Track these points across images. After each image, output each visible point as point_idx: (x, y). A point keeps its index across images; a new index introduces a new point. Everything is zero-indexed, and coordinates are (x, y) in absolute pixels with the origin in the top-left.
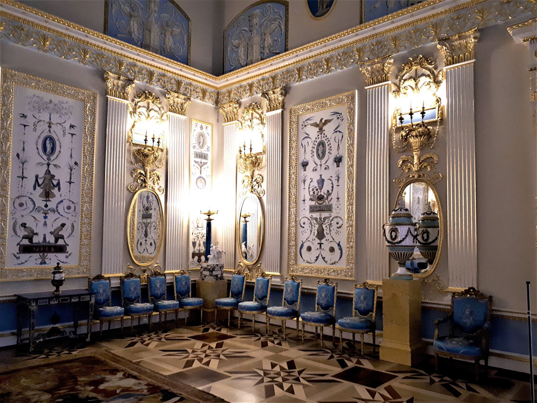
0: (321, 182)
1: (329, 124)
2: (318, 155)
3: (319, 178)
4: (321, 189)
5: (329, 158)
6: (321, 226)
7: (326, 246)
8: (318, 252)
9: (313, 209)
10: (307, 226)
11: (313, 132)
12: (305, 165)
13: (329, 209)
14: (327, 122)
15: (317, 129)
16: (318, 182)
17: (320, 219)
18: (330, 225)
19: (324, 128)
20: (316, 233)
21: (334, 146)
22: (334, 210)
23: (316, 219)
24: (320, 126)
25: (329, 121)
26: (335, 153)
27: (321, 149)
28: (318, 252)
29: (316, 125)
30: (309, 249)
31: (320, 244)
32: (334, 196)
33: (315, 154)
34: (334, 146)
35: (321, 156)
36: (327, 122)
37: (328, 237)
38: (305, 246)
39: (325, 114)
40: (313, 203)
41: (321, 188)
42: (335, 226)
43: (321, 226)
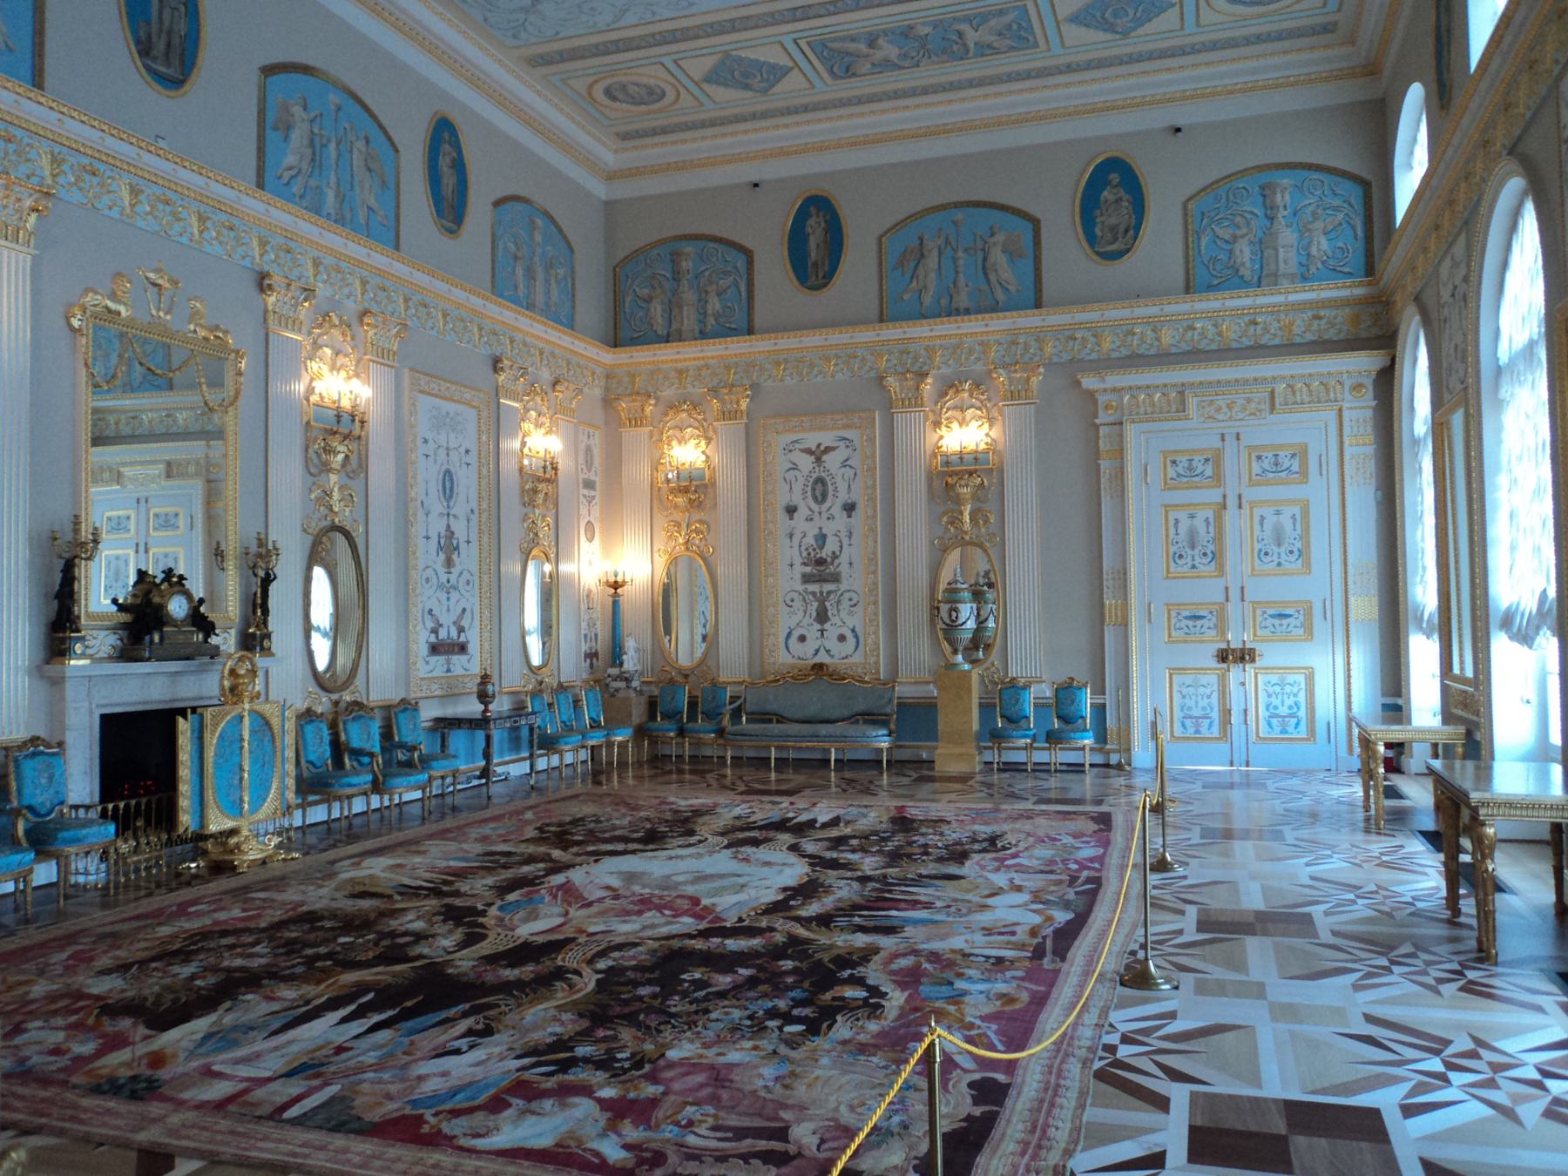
0: (821, 538)
1: (832, 454)
2: (815, 499)
3: (816, 531)
5: (835, 505)
7: (832, 631)
8: (819, 642)
9: (807, 579)
10: (798, 604)
11: (806, 462)
12: (791, 510)
13: (836, 578)
14: (828, 450)
15: (812, 458)
16: (816, 538)
18: (839, 602)
19: (824, 458)
21: (842, 486)
22: (844, 581)
23: (814, 594)
24: (818, 454)
26: (843, 496)
27: (820, 489)
28: (819, 642)
29: (809, 451)
30: (802, 639)
31: (822, 631)
32: (844, 559)
35: (821, 498)
36: (828, 450)
37: (834, 620)
38: (796, 634)
39: (827, 438)
40: (808, 569)
42: (845, 604)
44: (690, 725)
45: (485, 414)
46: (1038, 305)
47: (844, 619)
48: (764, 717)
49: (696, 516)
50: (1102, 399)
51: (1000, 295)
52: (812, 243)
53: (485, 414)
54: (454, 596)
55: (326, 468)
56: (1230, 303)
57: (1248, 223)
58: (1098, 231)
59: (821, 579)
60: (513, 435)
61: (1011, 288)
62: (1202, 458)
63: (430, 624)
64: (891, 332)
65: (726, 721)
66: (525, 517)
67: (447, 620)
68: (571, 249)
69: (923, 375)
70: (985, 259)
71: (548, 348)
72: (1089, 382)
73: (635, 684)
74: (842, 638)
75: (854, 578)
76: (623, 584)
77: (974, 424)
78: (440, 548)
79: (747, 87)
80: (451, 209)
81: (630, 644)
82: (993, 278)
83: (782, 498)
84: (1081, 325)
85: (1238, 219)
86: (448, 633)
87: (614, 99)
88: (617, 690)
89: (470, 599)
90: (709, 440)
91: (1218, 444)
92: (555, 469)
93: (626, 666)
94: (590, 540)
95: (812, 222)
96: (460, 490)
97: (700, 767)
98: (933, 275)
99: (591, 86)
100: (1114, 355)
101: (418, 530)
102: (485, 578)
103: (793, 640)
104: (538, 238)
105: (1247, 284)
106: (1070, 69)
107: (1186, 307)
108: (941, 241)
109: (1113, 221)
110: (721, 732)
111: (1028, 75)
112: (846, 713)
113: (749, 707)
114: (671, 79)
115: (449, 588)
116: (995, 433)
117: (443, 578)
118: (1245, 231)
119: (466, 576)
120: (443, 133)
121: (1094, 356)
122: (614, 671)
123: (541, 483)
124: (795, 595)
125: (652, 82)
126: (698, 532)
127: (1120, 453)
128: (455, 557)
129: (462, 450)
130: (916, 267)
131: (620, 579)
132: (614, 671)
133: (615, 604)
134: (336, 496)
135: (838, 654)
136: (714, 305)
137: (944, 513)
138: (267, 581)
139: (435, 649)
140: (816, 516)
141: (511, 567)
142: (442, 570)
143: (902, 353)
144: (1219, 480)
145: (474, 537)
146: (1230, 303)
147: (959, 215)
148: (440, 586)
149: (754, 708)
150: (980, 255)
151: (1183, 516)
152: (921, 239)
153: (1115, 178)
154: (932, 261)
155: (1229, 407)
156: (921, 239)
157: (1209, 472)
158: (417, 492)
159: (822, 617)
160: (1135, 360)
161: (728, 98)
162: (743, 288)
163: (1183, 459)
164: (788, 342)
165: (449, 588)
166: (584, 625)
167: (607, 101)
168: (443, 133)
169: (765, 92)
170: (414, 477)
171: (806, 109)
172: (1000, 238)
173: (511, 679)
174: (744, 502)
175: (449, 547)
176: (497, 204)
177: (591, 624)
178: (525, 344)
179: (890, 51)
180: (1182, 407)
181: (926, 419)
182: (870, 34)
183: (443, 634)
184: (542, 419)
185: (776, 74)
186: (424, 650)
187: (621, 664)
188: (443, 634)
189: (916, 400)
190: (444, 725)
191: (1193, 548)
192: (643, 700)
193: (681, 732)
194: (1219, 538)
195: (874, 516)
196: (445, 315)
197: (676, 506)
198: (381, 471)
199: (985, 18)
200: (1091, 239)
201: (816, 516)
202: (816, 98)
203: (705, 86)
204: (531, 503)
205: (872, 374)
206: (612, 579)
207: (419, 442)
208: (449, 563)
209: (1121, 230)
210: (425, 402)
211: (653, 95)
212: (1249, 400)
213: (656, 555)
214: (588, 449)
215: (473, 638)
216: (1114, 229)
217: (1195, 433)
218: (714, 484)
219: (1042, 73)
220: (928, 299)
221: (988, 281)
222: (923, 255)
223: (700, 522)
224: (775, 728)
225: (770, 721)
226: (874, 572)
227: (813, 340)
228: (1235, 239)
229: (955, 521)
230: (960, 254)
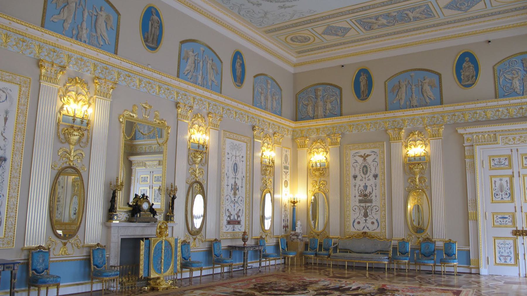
0: (366, 187)
1: (369, 157)
2: (363, 173)
3: (364, 184)
4: (366, 191)
5: (370, 175)
6: (366, 210)
7: (369, 221)
9: (360, 201)
10: (357, 210)
11: (360, 160)
12: (355, 177)
13: (371, 201)
14: (368, 156)
15: (363, 159)
16: (364, 187)
17: (366, 207)
18: (372, 210)
19: (367, 158)
20: (363, 214)
21: (373, 169)
22: (374, 202)
23: (363, 207)
24: (365, 157)
25: (370, 155)
26: (373, 172)
27: (365, 170)
29: (361, 156)
30: (359, 223)
31: (366, 220)
32: (373, 194)
33: (361, 171)
34: (373, 169)
35: (365, 173)
36: (368, 156)
37: (370, 216)
39: (367, 152)
40: (361, 198)
41: (366, 190)
42: (374, 211)
43: (366, 210)
44: (320, 252)
45: (249, 145)
46: (441, 103)
47: (374, 216)
48: (345, 251)
49: (322, 179)
50: (465, 137)
51: (428, 100)
52: (362, 84)
53: (249, 145)
54: (236, 205)
55: (194, 163)
56: (512, 102)
57: (517, 73)
58: (462, 77)
59: (365, 202)
60: (259, 151)
61: (432, 98)
62: (504, 158)
63: (228, 214)
64: (390, 114)
65: (331, 251)
66: (262, 179)
67: (234, 213)
68: (281, 90)
69: (401, 129)
70: (422, 88)
71: (271, 122)
72: (461, 131)
73: (300, 237)
74: (373, 223)
75: (377, 202)
76: (297, 202)
77: (420, 146)
78: (232, 189)
79: (337, 35)
80: (239, 78)
81: (299, 223)
82: (425, 94)
83: (352, 173)
84: (457, 111)
85: (514, 71)
86: (234, 217)
88: (294, 239)
89: (242, 206)
90: (327, 152)
91: (510, 153)
92: (273, 163)
93: (297, 231)
94: (286, 187)
95: (361, 77)
96: (240, 170)
97: (322, 266)
98: (404, 94)
100: (470, 121)
101: (225, 183)
102: (248, 199)
103: (356, 223)
104: (269, 87)
105: (519, 95)
107: (495, 103)
108: (407, 83)
109: (467, 74)
110: (329, 256)
112: (374, 250)
113: (339, 247)
115: (235, 202)
116: (428, 149)
117: (233, 199)
118: (516, 75)
119: (241, 198)
120: (238, 56)
121: (462, 121)
122: (293, 233)
123: (268, 168)
124: (356, 207)
125: (306, 35)
126: (322, 184)
127: (473, 157)
128: (237, 192)
129: (241, 157)
130: (398, 92)
131: (295, 200)
132: (293, 233)
133: (294, 209)
134: (197, 171)
135: (372, 229)
136: (329, 106)
137: (409, 178)
138: (174, 198)
139: (229, 223)
140: (364, 179)
141: (257, 196)
142: (232, 197)
143: (393, 121)
144: (510, 166)
145: (244, 185)
146: (512, 102)
147: (412, 74)
148: (232, 202)
149: (342, 248)
150: (420, 87)
151: (497, 179)
152: (399, 82)
153: (467, 59)
154: (403, 89)
155: (514, 139)
156: (399, 82)
157: (507, 163)
158: (225, 170)
159: (366, 215)
160: (477, 123)
161: (331, 39)
162: (339, 100)
163: (497, 159)
164: (353, 118)
165: (235, 202)
166: (283, 216)
167: (291, 42)
168: (238, 56)
169: (343, 36)
170: (224, 165)
171: (358, 41)
172: (427, 81)
173: (256, 233)
174: (339, 174)
175: (235, 189)
176: (255, 77)
177: (286, 216)
178: (263, 121)
179: (384, 21)
180: (496, 139)
181: (402, 144)
183: (232, 218)
184: (269, 146)
185: (346, 30)
186: (225, 222)
187: (295, 230)
188: (232, 218)
189: (399, 138)
190: (231, 249)
191: (502, 192)
192: (303, 243)
193: (316, 254)
194: (512, 188)
195: (384, 179)
196: (236, 113)
197: (316, 175)
198: (213, 163)
200: (460, 80)
201: (364, 179)
202: (361, 37)
203: (323, 35)
204: (265, 174)
205: (383, 129)
206: (293, 200)
207: (226, 154)
208: (235, 194)
209: (471, 76)
210: (228, 141)
211: (307, 39)
212: (521, 137)
213: (309, 192)
214: (286, 156)
215: (242, 219)
216: (467, 76)
217: (501, 149)
218: (328, 168)
219: (438, 25)
220: (402, 102)
221: (423, 95)
222: (400, 88)
223: (324, 181)
224: (348, 254)
225: (347, 252)
226: (385, 199)
227: (362, 117)
228: (513, 78)
229: (413, 181)
230: (413, 87)
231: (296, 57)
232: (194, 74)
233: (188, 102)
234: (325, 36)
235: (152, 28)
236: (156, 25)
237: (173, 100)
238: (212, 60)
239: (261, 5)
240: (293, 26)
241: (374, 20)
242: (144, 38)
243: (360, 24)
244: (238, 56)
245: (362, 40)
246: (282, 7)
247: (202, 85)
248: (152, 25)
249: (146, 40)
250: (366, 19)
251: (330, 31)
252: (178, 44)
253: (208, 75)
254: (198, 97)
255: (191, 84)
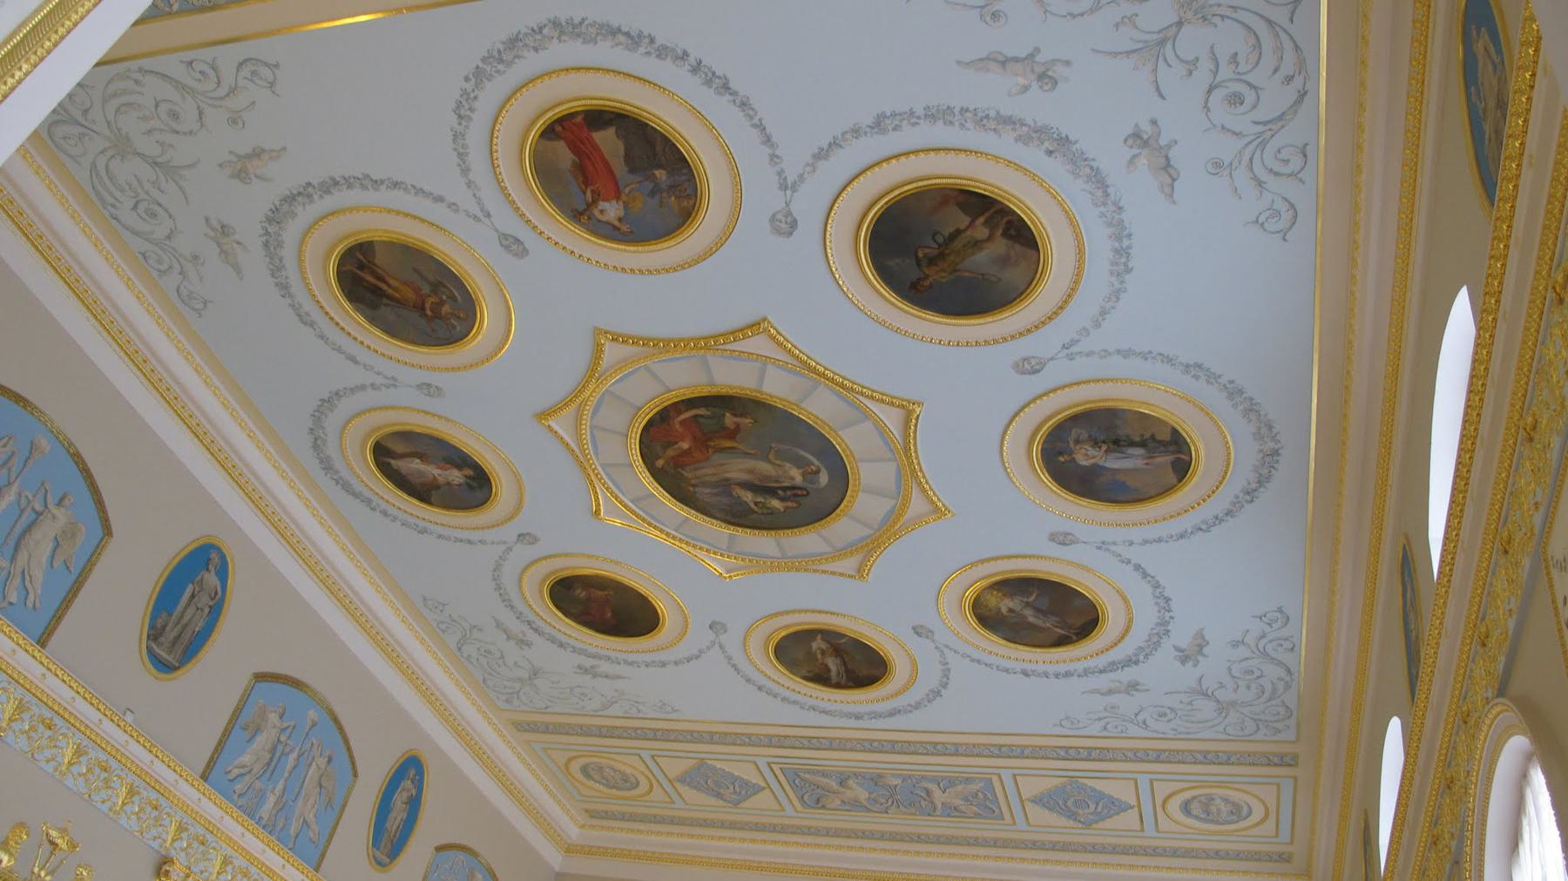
79: (719, 796)
87: (589, 776)
99: (570, 760)
106: (1035, 845)
111: (995, 843)
114: (643, 768)
120: (410, 769)
125: (628, 771)
161: (698, 802)
168: (410, 769)
171: (774, 829)
179: (863, 795)
182: (842, 773)
199: (952, 782)
203: (677, 785)
211: (628, 782)
231: (582, 826)
232: (258, 784)
233: (201, 866)
234: (683, 789)
235: (188, 604)
236: (204, 600)
237: (156, 845)
238: (330, 760)
239: (529, 644)
240: (602, 732)
241: (834, 784)
242: (152, 627)
243: (793, 784)
244: (412, 772)
245: (784, 829)
246: (584, 671)
247: (269, 827)
248: (193, 596)
249: (155, 634)
250: (809, 772)
251: (702, 778)
252: (245, 679)
253: (300, 802)
254: (240, 862)
255: (236, 813)
